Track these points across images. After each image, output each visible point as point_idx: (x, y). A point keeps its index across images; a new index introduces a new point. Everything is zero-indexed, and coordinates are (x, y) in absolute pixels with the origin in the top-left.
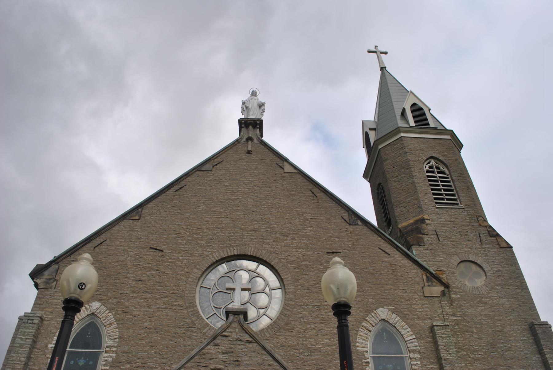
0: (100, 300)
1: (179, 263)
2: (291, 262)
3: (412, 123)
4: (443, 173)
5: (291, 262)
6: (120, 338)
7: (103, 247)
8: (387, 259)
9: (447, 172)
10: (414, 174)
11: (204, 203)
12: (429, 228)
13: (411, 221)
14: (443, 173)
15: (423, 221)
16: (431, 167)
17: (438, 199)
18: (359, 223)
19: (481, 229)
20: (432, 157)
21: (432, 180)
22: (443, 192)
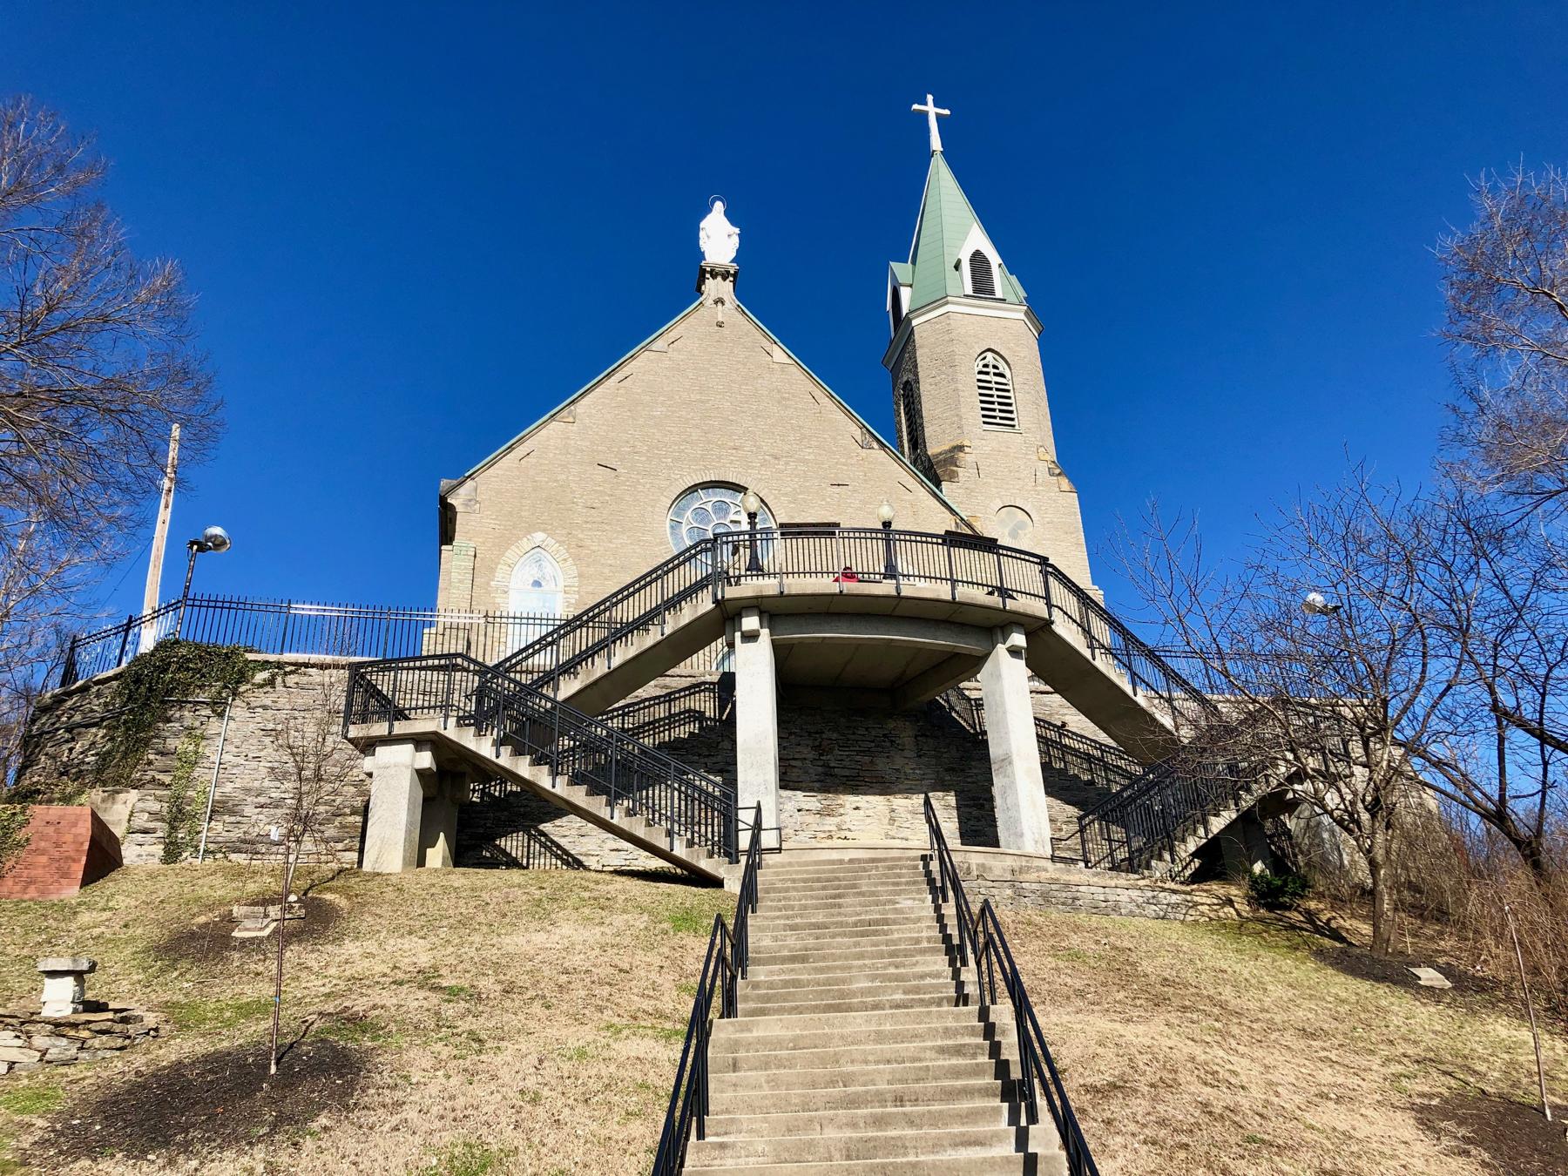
0: (544, 531)
1: (640, 488)
2: (786, 494)
3: (969, 290)
4: (1003, 376)
5: (786, 494)
6: (581, 575)
7: (531, 460)
8: (909, 497)
9: (1008, 374)
10: (960, 376)
11: (663, 403)
12: (966, 459)
13: (947, 448)
14: (1003, 376)
15: (960, 448)
16: (986, 366)
17: (988, 418)
18: (875, 445)
19: (1041, 464)
20: (989, 350)
21: (983, 386)
22: (996, 406)
